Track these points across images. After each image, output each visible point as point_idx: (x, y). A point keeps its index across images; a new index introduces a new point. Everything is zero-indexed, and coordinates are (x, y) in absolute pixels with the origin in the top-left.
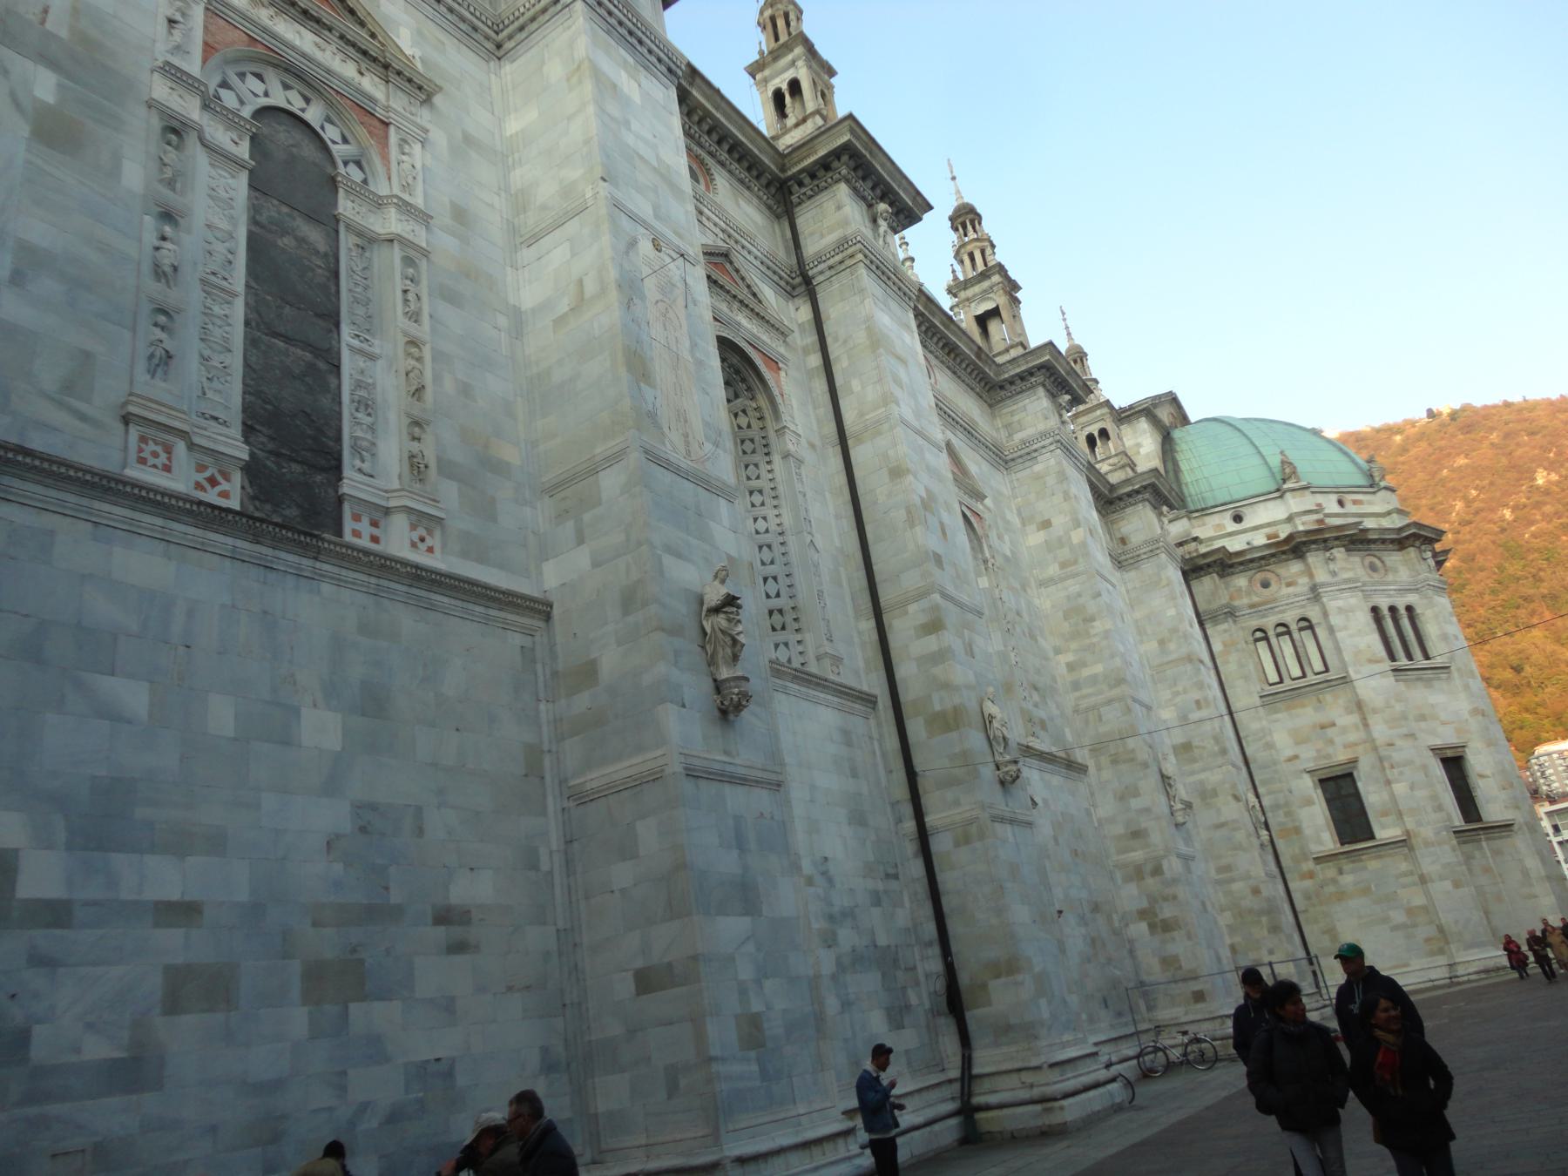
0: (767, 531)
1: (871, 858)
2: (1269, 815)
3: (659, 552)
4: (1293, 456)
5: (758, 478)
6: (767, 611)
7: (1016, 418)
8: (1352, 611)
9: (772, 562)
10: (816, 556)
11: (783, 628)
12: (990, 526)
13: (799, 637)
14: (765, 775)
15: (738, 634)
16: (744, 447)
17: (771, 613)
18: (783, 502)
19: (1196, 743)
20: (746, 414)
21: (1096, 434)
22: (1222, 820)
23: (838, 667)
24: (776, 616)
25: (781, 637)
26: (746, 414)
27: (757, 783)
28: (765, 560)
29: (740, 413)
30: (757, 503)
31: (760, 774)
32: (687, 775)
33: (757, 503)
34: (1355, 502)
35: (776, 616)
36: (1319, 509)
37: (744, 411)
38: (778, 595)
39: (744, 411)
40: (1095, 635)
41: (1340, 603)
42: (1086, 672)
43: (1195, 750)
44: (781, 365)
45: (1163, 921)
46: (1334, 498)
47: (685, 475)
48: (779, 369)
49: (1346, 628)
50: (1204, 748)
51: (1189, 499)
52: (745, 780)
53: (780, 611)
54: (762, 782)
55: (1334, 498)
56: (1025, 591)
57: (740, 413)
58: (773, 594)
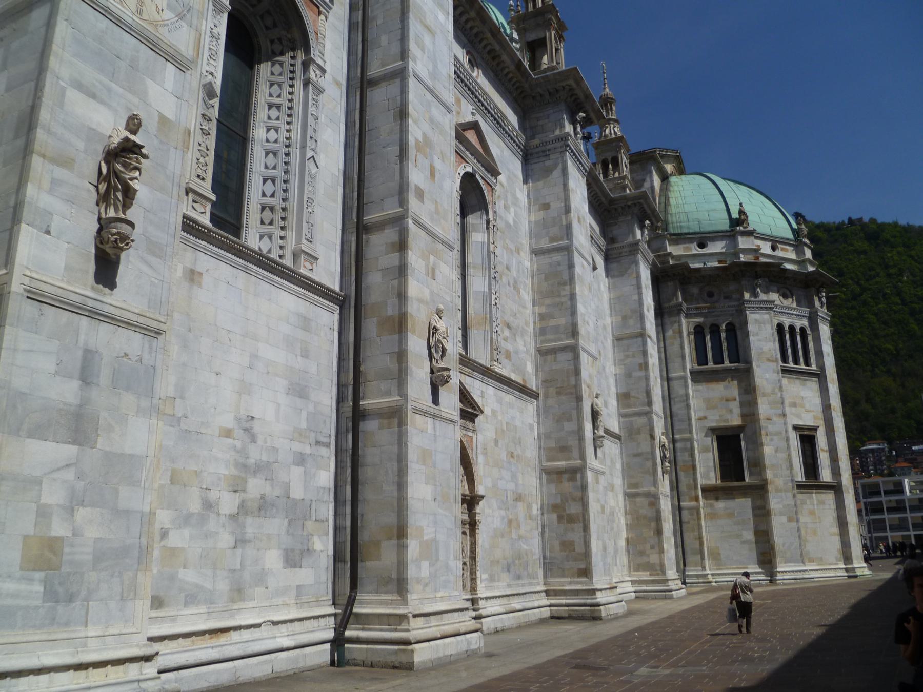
0: (276, 141)
1: (304, 425)
2: (679, 454)
3: (62, 83)
4: (746, 208)
5: (279, 96)
6: (260, 207)
7: (541, 123)
8: (764, 324)
9: (274, 168)
10: (314, 170)
11: (271, 223)
12: (499, 197)
13: (282, 233)
14: (141, 320)
15: (131, 179)
16: (273, 69)
17: (263, 208)
18: (295, 120)
19: (633, 394)
20: (281, 43)
21: (610, 159)
22: (640, 451)
23: (312, 264)
24: (267, 213)
25: (267, 229)
26: (281, 43)
27: (128, 324)
28: (268, 164)
29: (276, 41)
30: (274, 117)
31: (134, 318)
32: (28, 297)
33: (274, 117)
34: (782, 249)
35: (267, 213)
36: (756, 251)
37: (280, 40)
38: (273, 196)
39: (280, 40)
40: (564, 296)
41: (757, 316)
42: (552, 323)
43: (632, 399)
44: (321, 9)
45: (569, 515)
46: (769, 244)
47: (129, 29)
48: (320, 13)
49: (757, 334)
50: (638, 398)
51: (671, 225)
52: (113, 319)
53: (272, 209)
54: (136, 326)
55: (769, 244)
56: (519, 253)
57: (276, 41)
58: (268, 193)
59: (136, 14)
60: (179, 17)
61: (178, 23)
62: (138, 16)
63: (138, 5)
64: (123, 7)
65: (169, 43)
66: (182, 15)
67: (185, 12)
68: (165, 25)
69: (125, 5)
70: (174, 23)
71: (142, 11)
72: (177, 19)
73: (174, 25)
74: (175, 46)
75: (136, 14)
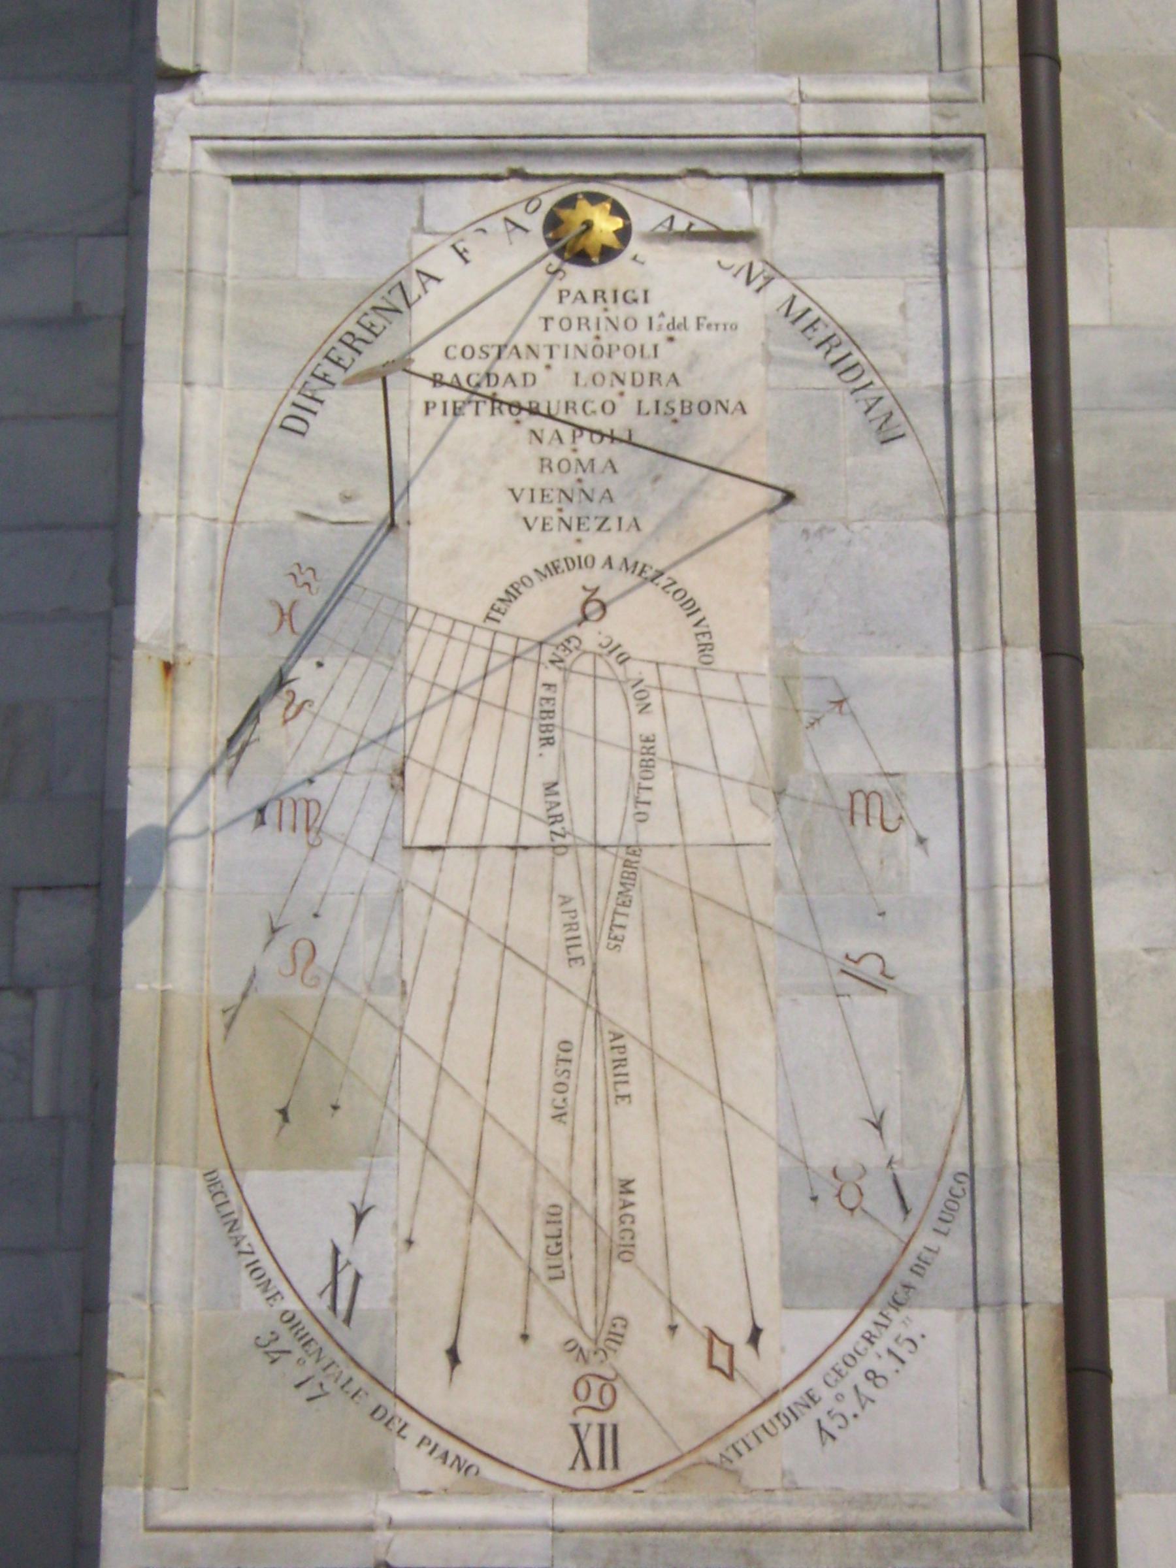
59: (579, 1478)
60: (883, 1298)
61: (881, 1345)
62: (597, 1478)
63: (584, 1417)
64: (489, 1490)
65: (826, 1515)
66: (903, 1273)
67: (925, 1239)
68: (791, 1416)
69: (491, 1471)
70: (853, 1357)
71: (611, 1437)
72: (871, 1314)
73: (856, 1375)
74: (867, 1500)
75: (579, 1478)
